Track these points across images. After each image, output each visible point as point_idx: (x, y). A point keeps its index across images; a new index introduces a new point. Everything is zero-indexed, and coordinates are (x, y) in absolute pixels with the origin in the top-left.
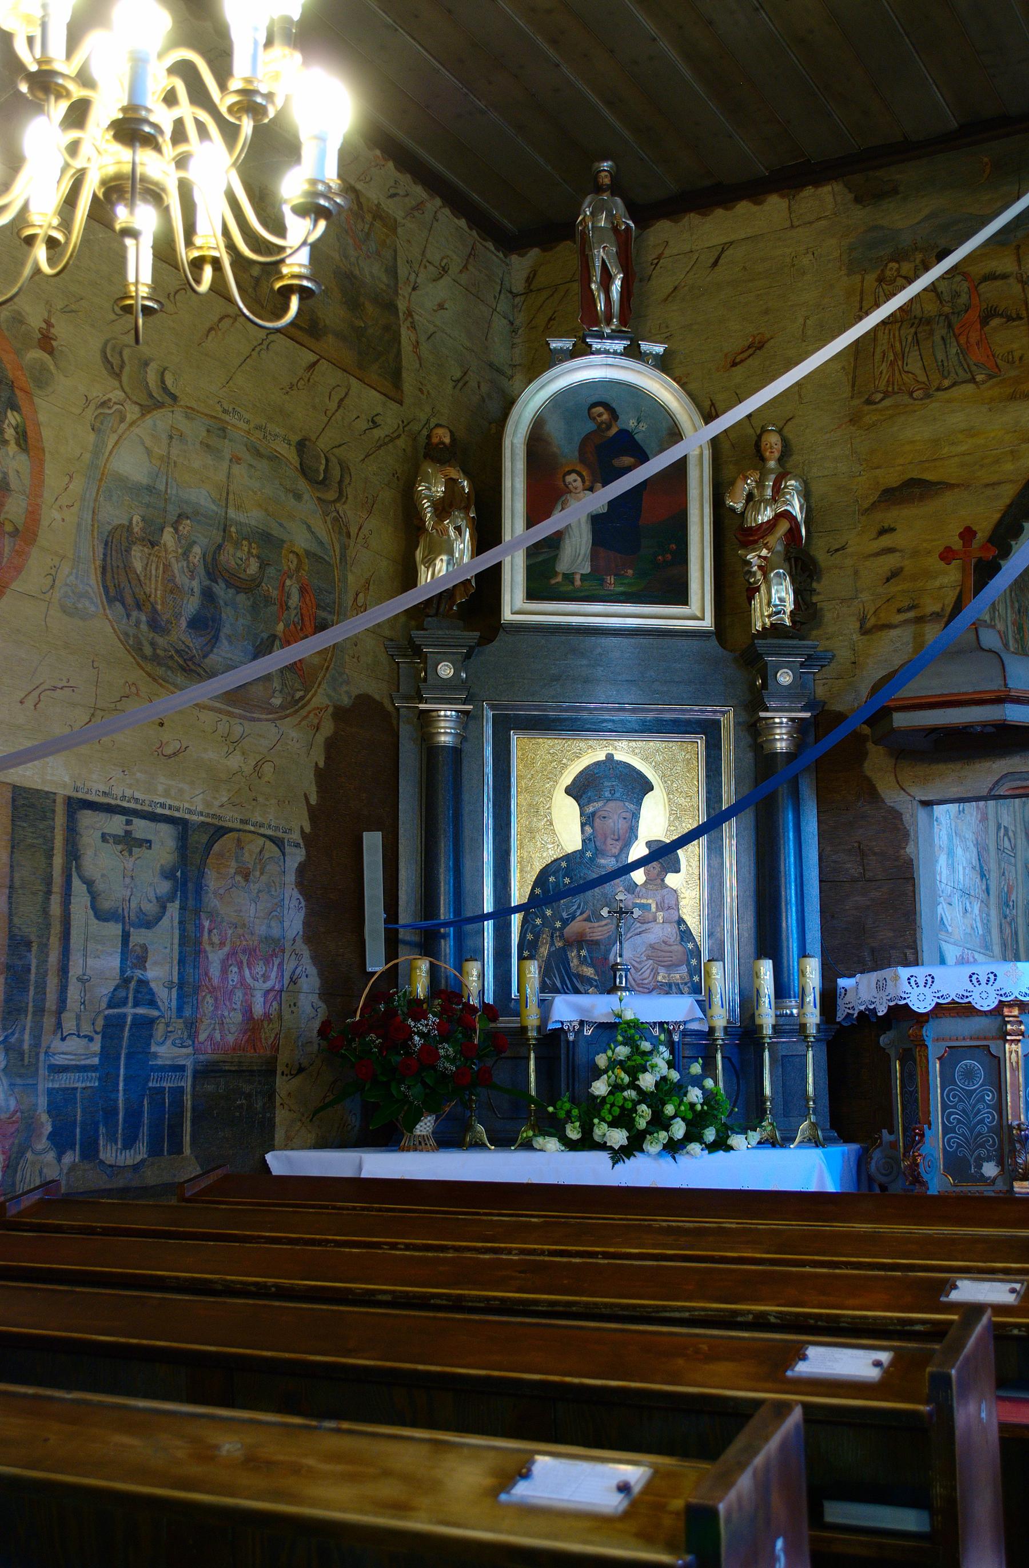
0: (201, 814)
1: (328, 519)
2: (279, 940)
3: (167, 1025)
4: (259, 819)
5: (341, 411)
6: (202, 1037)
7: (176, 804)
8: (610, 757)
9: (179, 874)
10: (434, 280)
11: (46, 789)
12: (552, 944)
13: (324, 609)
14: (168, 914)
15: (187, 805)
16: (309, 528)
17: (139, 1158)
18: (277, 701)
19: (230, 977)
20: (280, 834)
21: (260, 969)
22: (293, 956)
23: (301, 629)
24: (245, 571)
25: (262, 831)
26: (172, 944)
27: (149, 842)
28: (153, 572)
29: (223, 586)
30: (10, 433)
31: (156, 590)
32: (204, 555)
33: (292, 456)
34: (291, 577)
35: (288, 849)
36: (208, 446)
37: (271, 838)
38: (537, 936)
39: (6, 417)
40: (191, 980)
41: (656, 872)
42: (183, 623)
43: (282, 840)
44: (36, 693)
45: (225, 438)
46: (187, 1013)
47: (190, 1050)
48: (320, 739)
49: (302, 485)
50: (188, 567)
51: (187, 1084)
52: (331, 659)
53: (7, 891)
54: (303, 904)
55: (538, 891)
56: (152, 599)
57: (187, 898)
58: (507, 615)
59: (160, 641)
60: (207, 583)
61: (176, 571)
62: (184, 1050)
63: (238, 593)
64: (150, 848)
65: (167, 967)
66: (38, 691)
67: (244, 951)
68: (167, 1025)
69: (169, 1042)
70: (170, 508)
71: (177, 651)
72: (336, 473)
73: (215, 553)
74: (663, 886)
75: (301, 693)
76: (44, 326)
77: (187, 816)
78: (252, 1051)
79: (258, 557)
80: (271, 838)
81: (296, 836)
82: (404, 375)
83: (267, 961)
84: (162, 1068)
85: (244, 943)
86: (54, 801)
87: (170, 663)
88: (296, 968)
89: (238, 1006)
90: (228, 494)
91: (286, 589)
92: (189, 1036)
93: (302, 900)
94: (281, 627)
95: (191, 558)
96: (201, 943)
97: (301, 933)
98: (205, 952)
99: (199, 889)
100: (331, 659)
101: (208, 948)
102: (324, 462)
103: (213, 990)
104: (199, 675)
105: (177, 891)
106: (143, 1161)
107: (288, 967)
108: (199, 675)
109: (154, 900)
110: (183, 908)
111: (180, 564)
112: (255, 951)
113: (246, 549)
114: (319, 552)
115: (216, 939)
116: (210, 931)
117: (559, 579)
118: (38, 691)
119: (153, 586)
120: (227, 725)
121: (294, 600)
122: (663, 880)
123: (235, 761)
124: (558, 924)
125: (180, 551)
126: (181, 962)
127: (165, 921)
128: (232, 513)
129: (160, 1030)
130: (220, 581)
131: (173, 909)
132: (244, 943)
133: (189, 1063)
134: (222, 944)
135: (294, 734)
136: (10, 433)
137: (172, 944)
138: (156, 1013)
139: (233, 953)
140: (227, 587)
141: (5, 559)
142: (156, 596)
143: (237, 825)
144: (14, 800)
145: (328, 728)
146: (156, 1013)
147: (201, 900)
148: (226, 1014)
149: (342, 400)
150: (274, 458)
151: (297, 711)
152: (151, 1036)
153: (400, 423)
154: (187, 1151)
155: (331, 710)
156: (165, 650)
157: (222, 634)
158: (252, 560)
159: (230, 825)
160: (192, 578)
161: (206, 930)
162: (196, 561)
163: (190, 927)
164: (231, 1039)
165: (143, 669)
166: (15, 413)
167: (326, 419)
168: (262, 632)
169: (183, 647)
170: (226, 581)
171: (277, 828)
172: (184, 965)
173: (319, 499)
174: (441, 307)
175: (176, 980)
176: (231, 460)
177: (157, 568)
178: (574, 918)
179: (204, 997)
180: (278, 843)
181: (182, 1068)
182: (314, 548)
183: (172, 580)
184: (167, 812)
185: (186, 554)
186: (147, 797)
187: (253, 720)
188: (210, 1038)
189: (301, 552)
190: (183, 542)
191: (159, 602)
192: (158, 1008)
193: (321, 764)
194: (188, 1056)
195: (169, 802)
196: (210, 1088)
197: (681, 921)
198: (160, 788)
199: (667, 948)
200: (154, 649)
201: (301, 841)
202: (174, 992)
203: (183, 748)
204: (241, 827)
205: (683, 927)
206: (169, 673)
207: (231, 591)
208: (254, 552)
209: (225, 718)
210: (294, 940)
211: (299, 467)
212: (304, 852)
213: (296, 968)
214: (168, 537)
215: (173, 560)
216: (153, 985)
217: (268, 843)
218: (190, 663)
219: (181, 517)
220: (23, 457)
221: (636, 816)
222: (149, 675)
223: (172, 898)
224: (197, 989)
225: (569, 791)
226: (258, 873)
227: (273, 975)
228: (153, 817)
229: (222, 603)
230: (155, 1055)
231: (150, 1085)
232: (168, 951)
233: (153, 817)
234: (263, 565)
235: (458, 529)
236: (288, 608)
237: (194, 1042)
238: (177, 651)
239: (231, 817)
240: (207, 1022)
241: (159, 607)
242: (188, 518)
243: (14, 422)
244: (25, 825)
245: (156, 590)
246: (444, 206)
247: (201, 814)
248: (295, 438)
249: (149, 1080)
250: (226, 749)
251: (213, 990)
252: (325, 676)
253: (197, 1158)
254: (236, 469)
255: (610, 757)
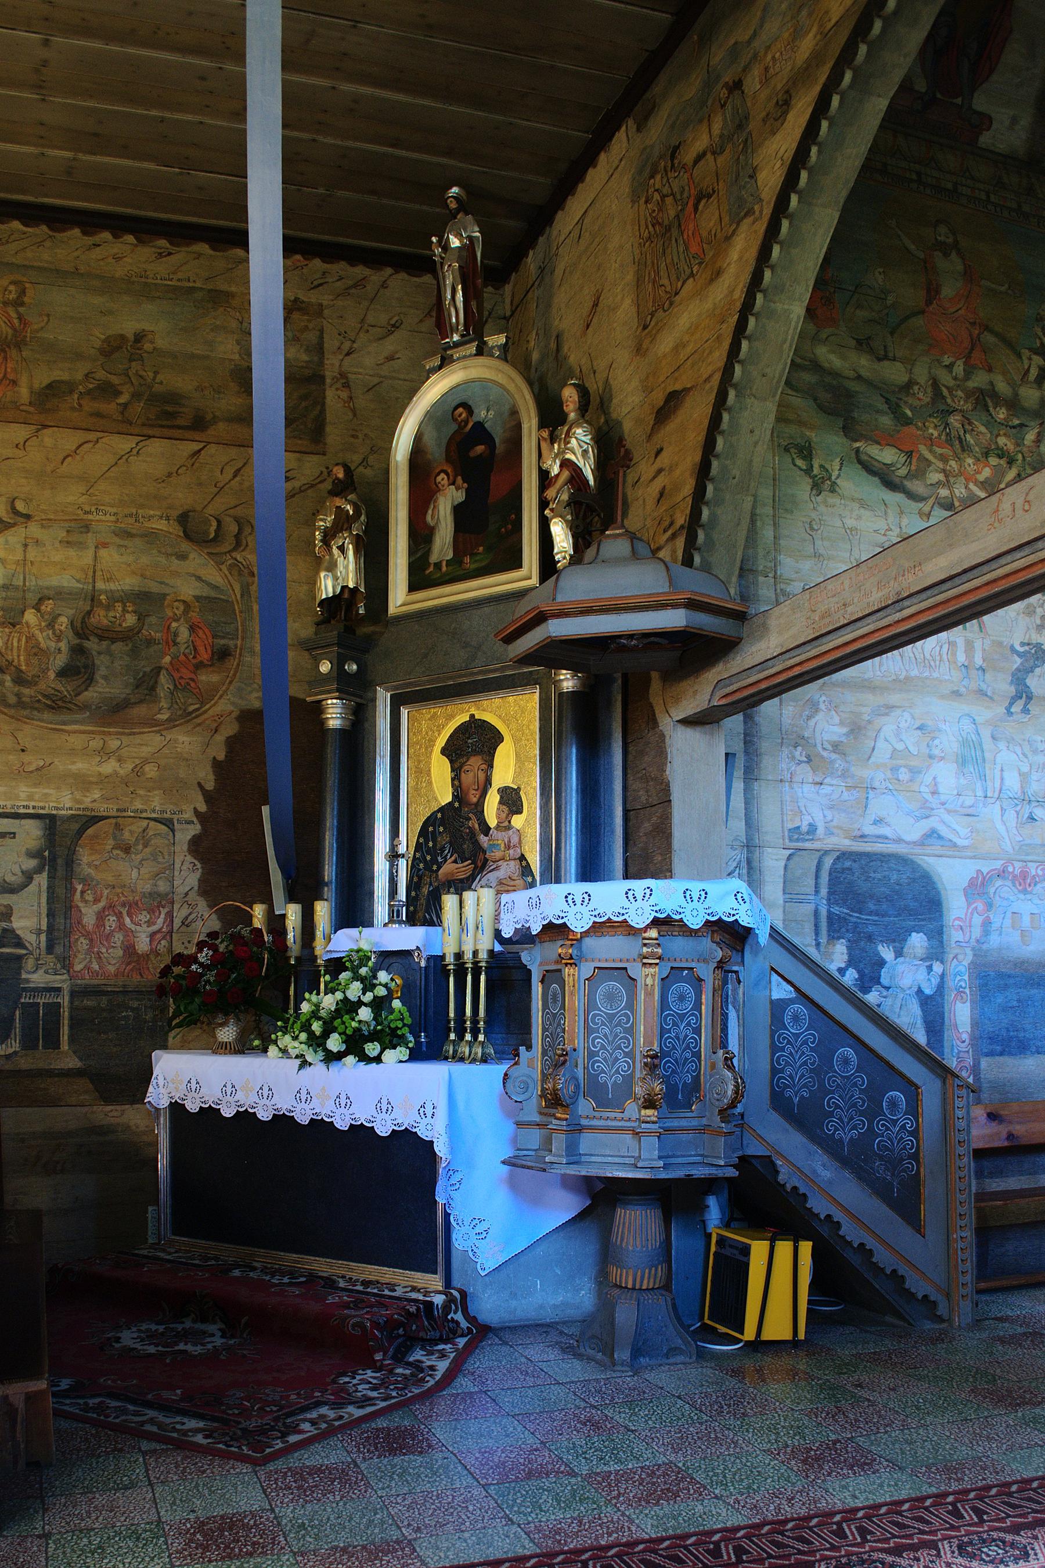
0: (71, 809)
1: (224, 568)
2: (167, 894)
3: (38, 959)
4: (140, 807)
5: (238, 479)
6: (78, 967)
7: (41, 804)
8: (472, 716)
9: (46, 853)
10: (380, 339)
12: (431, 884)
13: (223, 638)
14: (35, 882)
15: (52, 804)
16: (199, 578)
17: (10, 1051)
18: (164, 717)
19: (107, 924)
20: (167, 816)
21: (144, 917)
22: (185, 906)
23: (194, 657)
24: (120, 625)
25: (144, 815)
26: (39, 903)
27: (14, 833)
28: (15, 644)
29: (96, 640)
31: (19, 656)
32: (72, 623)
33: (177, 530)
34: (177, 620)
35: (177, 826)
36: (68, 542)
37: (155, 820)
38: (420, 878)
40: (62, 928)
41: (504, 815)
42: (52, 675)
43: (171, 821)
45: (87, 532)
46: (59, 950)
47: (65, 977)
48: (220, 738)
49: (185, 546)
50: (54, 633)
51: (65, 1000)
52: (235, 675)
54: (199, 866)
55: (421, 840)
56: (16, 663)
57: (56, 870)
58: (392, 610)
59: (27, 691)
60: (78, 641)
61: (41, 639)
62: (58, 977)
63: (113, 643)
64: (14, 837)
65: (35, 920)
67: (124, 905)
68: (38, 959)
69: (41, 972)
70: (29, 595)
71: (45, 696)
72: (234, 528)
73: (84, 618)
74: (509, 827)
75: (196, 706)
77: (54, 812)
78: (139, 977)
79: (135, 612)
80: (155, 820)
81: (189, 815)
82: (328, 429)
83: (151, 911)
84: (37, 991)
85: (123, 898)
87: (37, 705)
88: (190, 914)
89: (119, 944)
90: (94, 572)
91: (172, 630)
92: (63, 967)
93: (197, 862)
94: (168, 659)
95: (57, 627)
96: (72, 901)
97: (196, 888)
98: (78, 906)
99: (70, 863)
100: (235, 675)
101: (80, 904)
102: (215, 524)
103: (87, 935)
104: (68, 709)
105: (45, 865)
106: (15, 1053)
107: (179, 917)
108: (68, 709)
109: (20, 874)
110: (51, 877)
111: (45, 634)
112: (137, 904)
113: (120, 609)
114: (213, 594)
115: (89, 896)
116: (83, 892)
117: (431, 569)
119: (15, 654)
120: (102, 742)
121: (184, 634)
122: (510, 822)
123: (109, 767)
124: (435, 867)
125: (43, 624)
126: (51, 914)
127: (32, 887)
128: (100, 585)
129: (30, 963)
130: (91, 638)
131: (42, 880)
132: (123, 898)
133: (66, 986)
134: (96, 901)
135: (186, 739)
137: (39, 903)
138: (24, 952)
139: (111, 906)
140: (101, 640)
142: (19, 660)
143: (115, 814)
145: (230, 729)
146: (24, 952)
147: (72, 870)
148: (104, 950)
149: (239, 470)
150: (150, 537)
151: (188, 721)
152: (20, 968)
153: (324, 470)
154: (65, 1046)
155: (234, 715)
156: (31, 697)
157: (97, 677)
158: (128, 616)
159: (105, 814)
160: (59, 640)
161: (79, 891)
162: (62, 628)
163: (60, 891)
164: (112, 969)
165: (5, 714)
167: (217, 490)
168: (144, 667)
169: (53, 692)
170: (96, 635)
171: (163, 812)
172: (54, 916)
173: (209, 554)
174: (391, 358)
175: (44, 927)
176: (96, 547)
177: (19, 640)
178: (446, 861)
179: (77, 939)
180: (168, 823)
181: (58, 990)
182: (206, 592)
183: (37, 645)
184: (31, 811)
185: (51, 625)
186: (9, 803)
187: (134, 734)
188: (88, 968)
189: (188, 599)
190: (46, 617)
191: (23, 664)
192: (26, 948)
193: (221, 756)
194: (63, 981)
195: (32, 804)
196: (88, 1003)
197: (522, 858)
198: (23, 795)
199: (512, 883)
200: (20, 698)
201: (195, 820)
202: (43, 937)
203: (47, 764)
204: (119, 814)
205: (524, 863)
206: (35, 713)
207: (105, 643)
208: (130, 609)
209: (97, 737)
210: (187, 894)
211: (182, 534)
212: (198, 827)
213: (190, 914)
214: (30, 617)
215: (37, 632)
216: (18, 932)
217: (152, 824)
218: (60, 703)
219: (41, 600)
221: (491, 766)
222: (12, 717)
223: (39, 870)
224: (68, 934)
225: (444, 751)
226: (140, 847)
227: (160, 921)
228: (16, 816)
229: (94, 653)
230: (28, 981)
231: (23, 1000)
232: (35, 908)
233: (16, 816)
234: (141, 618)
235: (342, 549)
236: (175, 644)
237: (69, 971)
238: (45, 696)
239: (102, 809)
240: (80, 956)
241: (24, 668)
242: (49, 599)
245: (19, 656)
246: (397, 272)
247: (71, 809)
248: (176, 513)
249: (21, 997)
250: (99, 759)
251: (87, 935)
252: (228, 689)
253: (74, 1052)
254: (103, 553)
255: (472, 716)
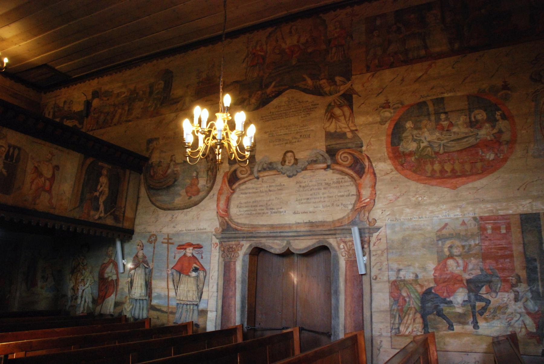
11: (534, 212)
30: (498, 117)
39: (496, 114)
44: (524, 186)
53: (522, 245)
66: (525, 184)
76: (503, 83)
86: (539, 215)
118: (525, 184)
136: (498, 117)
141: (505, 152)
144: (521, 218)
166: (499, 112)
220: (506, 122)
243: (499, 114)
244: (526, 224)
